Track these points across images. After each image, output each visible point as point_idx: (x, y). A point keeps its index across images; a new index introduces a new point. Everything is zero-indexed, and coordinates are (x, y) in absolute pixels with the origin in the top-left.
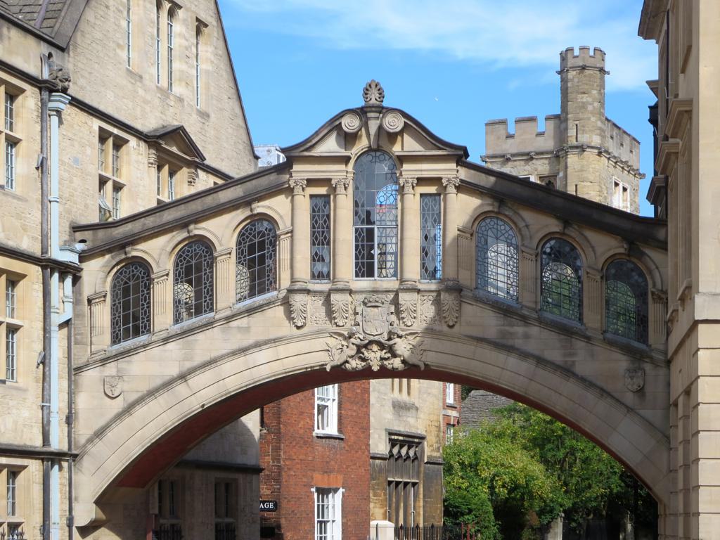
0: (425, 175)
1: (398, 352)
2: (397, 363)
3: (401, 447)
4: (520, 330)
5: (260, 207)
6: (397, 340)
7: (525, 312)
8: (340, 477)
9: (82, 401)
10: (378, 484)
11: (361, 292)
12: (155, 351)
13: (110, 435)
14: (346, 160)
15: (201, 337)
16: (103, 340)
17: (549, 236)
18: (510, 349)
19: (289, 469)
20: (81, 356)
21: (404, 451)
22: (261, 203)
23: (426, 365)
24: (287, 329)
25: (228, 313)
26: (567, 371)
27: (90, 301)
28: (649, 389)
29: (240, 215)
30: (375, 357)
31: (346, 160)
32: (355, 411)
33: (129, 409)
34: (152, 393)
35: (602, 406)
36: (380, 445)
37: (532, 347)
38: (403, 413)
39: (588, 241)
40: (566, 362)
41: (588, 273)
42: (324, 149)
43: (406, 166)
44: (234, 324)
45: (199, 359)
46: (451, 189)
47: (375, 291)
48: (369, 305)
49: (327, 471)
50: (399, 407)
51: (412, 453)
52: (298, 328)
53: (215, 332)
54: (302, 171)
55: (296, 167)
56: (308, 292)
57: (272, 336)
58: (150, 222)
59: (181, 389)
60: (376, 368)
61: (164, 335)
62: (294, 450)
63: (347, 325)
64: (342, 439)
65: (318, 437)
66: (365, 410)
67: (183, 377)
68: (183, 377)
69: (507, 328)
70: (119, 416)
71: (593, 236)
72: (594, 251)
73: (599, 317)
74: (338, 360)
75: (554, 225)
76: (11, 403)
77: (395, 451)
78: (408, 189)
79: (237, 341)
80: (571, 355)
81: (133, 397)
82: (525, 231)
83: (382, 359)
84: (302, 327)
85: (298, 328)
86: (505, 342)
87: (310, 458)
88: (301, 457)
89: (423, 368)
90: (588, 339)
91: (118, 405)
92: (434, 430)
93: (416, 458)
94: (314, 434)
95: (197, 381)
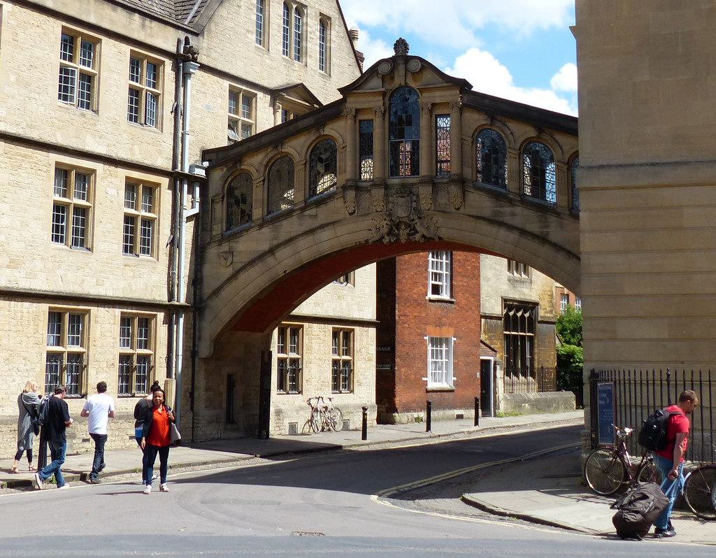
0: (438, 101)
1: (418, 229)
3: (518, 311)
4: (507, 209)
6: (417, 221)
8: (452, 330)
9: (208, 270)
10: (493, 336)
12: (254, 233)
13: (224, 293)
15: (285, 223)
16: (218, 229)
17: (529, 141)
18: (501, 224)
19: (404, 323)
21: (519, 314)
23: (440, 238)
26: (543, 239)
31: (384, 94)
32: (466, 282)
33: (234, 276)
34: (251, 263)
36: (497, 309)
37: (517, 222)
38: (518, 285)
39: (557, 142)
40: (542, 232)
43: (424, 95)
44: (307, 213)
45: (283, 237)
48: (398, 195)
49: (439, 324)
50: (512, 282)
51: (527, 315)
53: (294, 219)
55: (349, 100)
57: (332, 220)
59: (270, 260)
60: (403, 241)
61: (260, 222)
62: (409, 309)
64: (452, 303)
65: (430, 301)
66: (475, 281)
67: (272, 251)
68: (272, 251)
69: (498, 209)
71: (559, 137)
72: (562, 150)
73: (566, 198)
74: (377, 237)
75: (530, 132)
76: (143, 270)
77: (511, 313)
79: (308, 224)
80: (546, 227)
81: (240, 266)
83: (409, 235)
86: (497, 219)
87: (423, 315)
88: (415, 314)
89: (437, 240)
90: (558, 214)
91: (229, 272)
92: (547, 298)
93: (530, 318)
94: (427, 298)
95: (283, 253)
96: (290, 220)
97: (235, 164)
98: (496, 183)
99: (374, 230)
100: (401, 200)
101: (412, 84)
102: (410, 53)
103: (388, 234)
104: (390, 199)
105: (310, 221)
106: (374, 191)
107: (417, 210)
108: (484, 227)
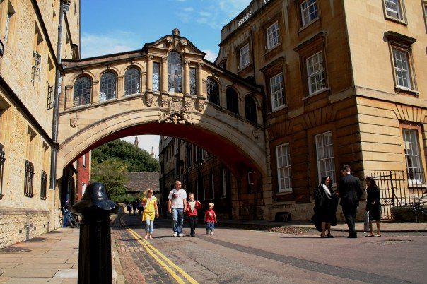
2: (183, 122)
5: (135, 63)
11: (171, 96)
13: (72, 141)
20: (62, 110)
25: (122, 98)
26: (237, 130)
27: (66, 88)
29: (129, 64)
30: (176, 119)
31: (166, 51)
33: (81, 132)
34: (91, 126)
37: (225, 120)
42: (161, 46)
53: (117, 105)
59: (103, 125)
63: (166, 107)
67: (104, 120)
68: (104, 120)
70: (77, 134)
74: (163, 119)
85: (148, 106)
90: (242, 119)
91: (76, 130)
95: (109, 123)
96: (114, 105)
100: (175, 103)
103: (168, 118)
106: (163, 97)
108: (214, 122)
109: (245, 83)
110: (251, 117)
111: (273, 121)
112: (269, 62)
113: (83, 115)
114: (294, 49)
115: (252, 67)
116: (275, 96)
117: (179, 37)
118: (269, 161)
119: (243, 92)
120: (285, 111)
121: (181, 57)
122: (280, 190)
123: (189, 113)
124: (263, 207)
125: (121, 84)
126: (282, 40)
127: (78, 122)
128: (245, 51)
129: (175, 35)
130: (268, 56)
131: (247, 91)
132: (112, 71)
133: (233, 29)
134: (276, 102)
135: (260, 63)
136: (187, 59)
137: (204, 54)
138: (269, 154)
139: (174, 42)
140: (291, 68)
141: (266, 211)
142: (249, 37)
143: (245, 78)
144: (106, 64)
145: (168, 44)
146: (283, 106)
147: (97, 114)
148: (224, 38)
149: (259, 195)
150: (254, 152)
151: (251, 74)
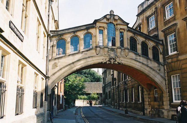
0: (121, 28)
4: (138, 58)
7: (139, 54)
14: (107, 23)
18: (137, 61)
22: (90, 30)
23: (122, 63)
24: (95, 54)
26: (148, 66)
28: (161, 70)
29: (86, 32)
30: (112, 61)
31: (107, 23)
35: (153, 72)
37: (141, 61)
41: (149, 48)
43: (118, 26)
46: (126, 31)
47: (112, 48)
52: (97, 54)
54: (98, 24)
55: (97, 24)
56: (100, 48)
58: (66, 31)
68: (73, 63)
71: (150, 42)
74: (105, 61)
75: (144, 40)
78: (118, 30)
80: (148, 63)
82: (139, 40)
83: (114, 62)
84: (98, 54)
85: (97, 54)
86: (136, 60)
90: (151, 60)
97: (61, 36)
98: (134, 51)
99: (104, 60)
101: (115, 23)
102: (115, 14)
104: (109, 52)
105: (85, 55)
107: (116, 56)
109: (153, 39)
110: (156, 58)
111: (170, 61)
112: (167, 27)
113: (61, 60)
114: (183, 19)
115: (156, 29)
116: (171, 46)
117: (114, 15)
118: (167, 84)
119: (151, 44)
120: (178, 55)
121: (115, 26)
122: (174, 101)
123: (120, 57)
124: (163, 110)
125: (82, 42)
126: (175, 13)
127: (59, 64)
128: (152, 19)
129: (112, 14)
130: (166, 23)
131: (154, 44)
132: (77, 36)
133: (145, 6)
134: (171, 50)
135: (162, 27)
136: (119, 27)
137: (128, 24)
138: (167, 79)
139: (111, 18)
140: (181, 30)
141: (165, 113)
142: (155, 11)
143: (151, 35)
144: (74, 32)
145: (108, 20)
146: (176, 52)
147: (71, 60)
148: (140, 11)
149: (161, 103)
150: (158, 79)
151: (156, 33)
